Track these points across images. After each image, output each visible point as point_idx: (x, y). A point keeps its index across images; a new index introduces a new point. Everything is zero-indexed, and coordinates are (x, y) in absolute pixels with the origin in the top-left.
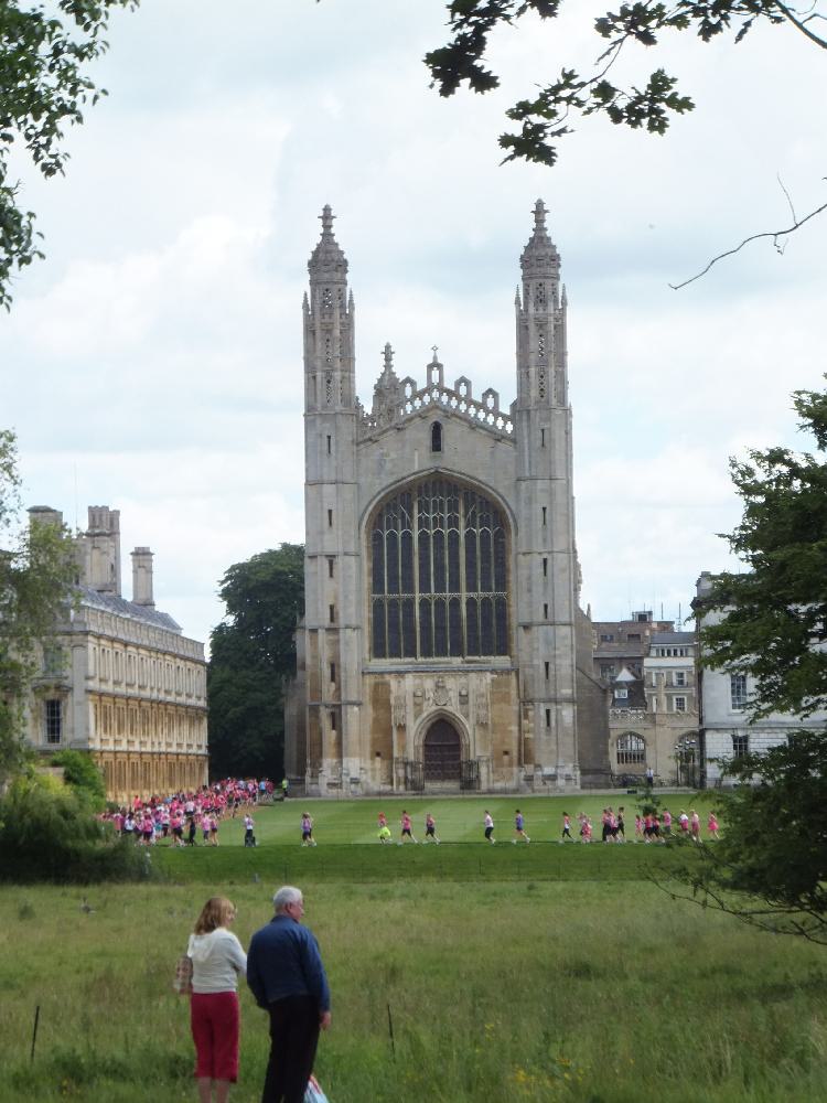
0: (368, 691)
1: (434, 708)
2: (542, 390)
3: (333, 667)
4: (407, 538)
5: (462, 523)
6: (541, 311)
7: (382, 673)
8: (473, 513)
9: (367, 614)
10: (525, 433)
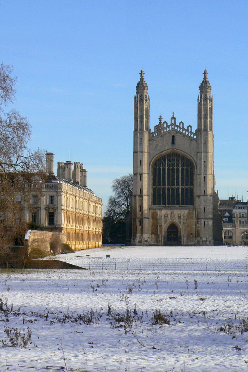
0: (151, 214)
1: (171, 220)
2: (205, 126)
4: (164, 169)
5: (180, 165)
6: (205, 103)
7: (155, 209)
10: (200, 138)
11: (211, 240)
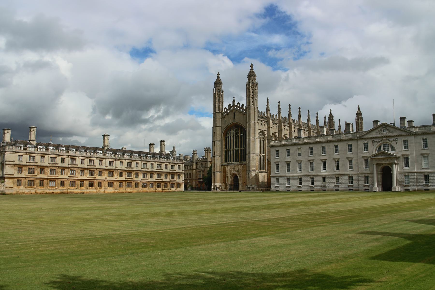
1: (233, 173)
3: (214, 164)
5: (240, 133)
8: (242, 131)
11: (254, 187)
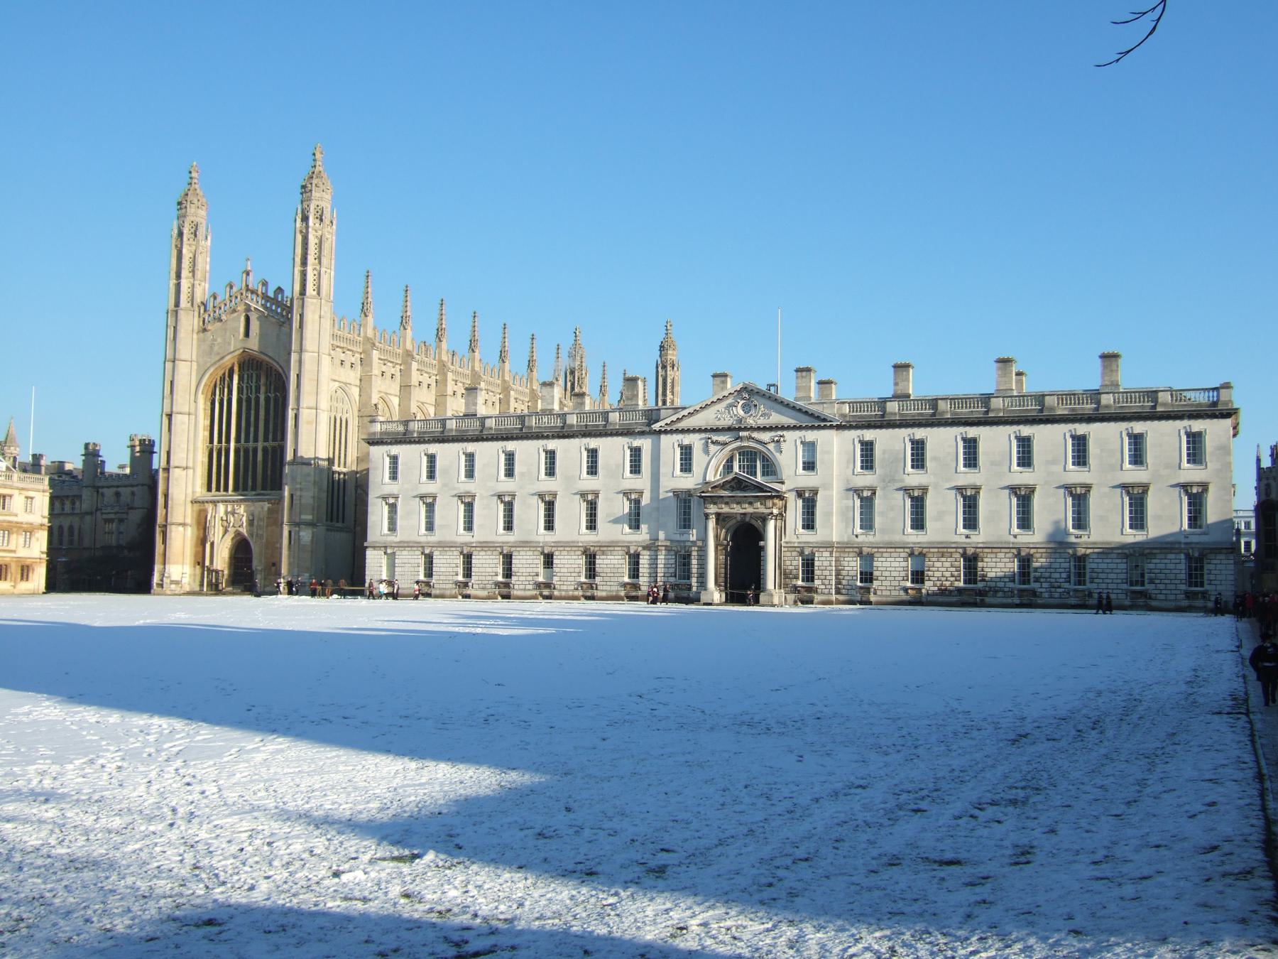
5: (263, 389)
7: (203, 502)
9: (202, 458)
